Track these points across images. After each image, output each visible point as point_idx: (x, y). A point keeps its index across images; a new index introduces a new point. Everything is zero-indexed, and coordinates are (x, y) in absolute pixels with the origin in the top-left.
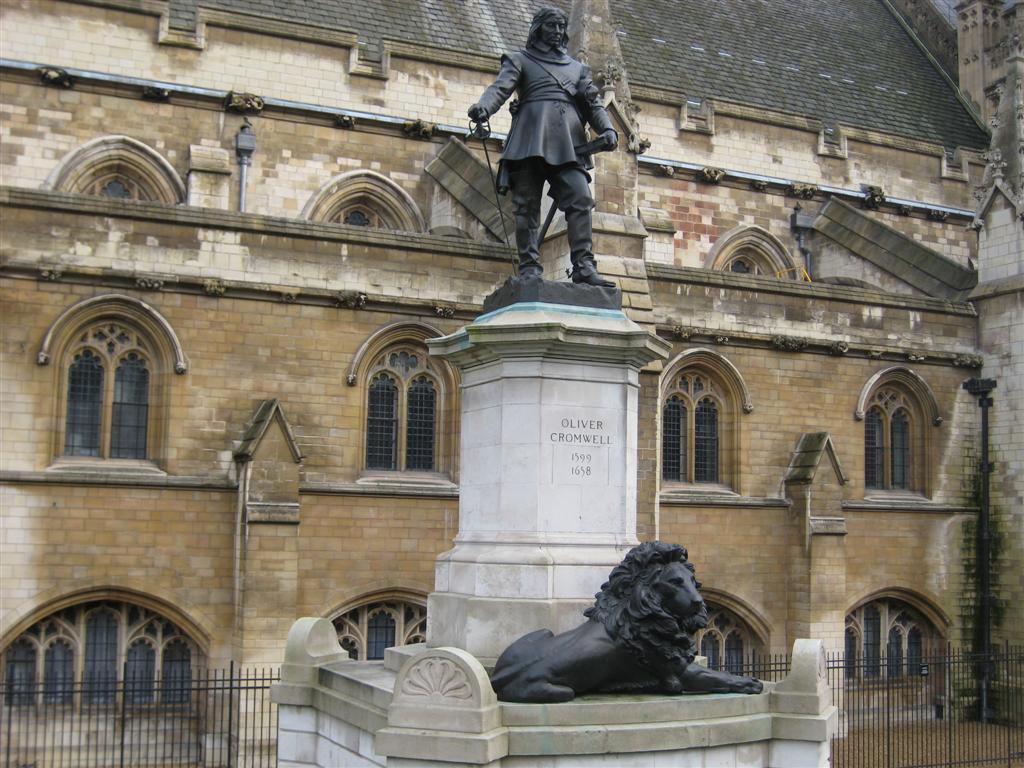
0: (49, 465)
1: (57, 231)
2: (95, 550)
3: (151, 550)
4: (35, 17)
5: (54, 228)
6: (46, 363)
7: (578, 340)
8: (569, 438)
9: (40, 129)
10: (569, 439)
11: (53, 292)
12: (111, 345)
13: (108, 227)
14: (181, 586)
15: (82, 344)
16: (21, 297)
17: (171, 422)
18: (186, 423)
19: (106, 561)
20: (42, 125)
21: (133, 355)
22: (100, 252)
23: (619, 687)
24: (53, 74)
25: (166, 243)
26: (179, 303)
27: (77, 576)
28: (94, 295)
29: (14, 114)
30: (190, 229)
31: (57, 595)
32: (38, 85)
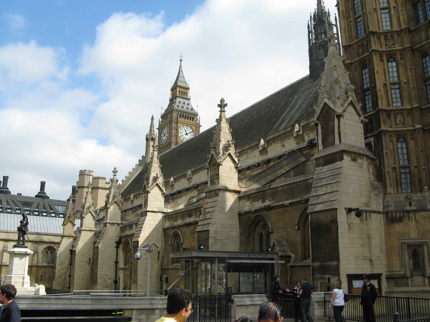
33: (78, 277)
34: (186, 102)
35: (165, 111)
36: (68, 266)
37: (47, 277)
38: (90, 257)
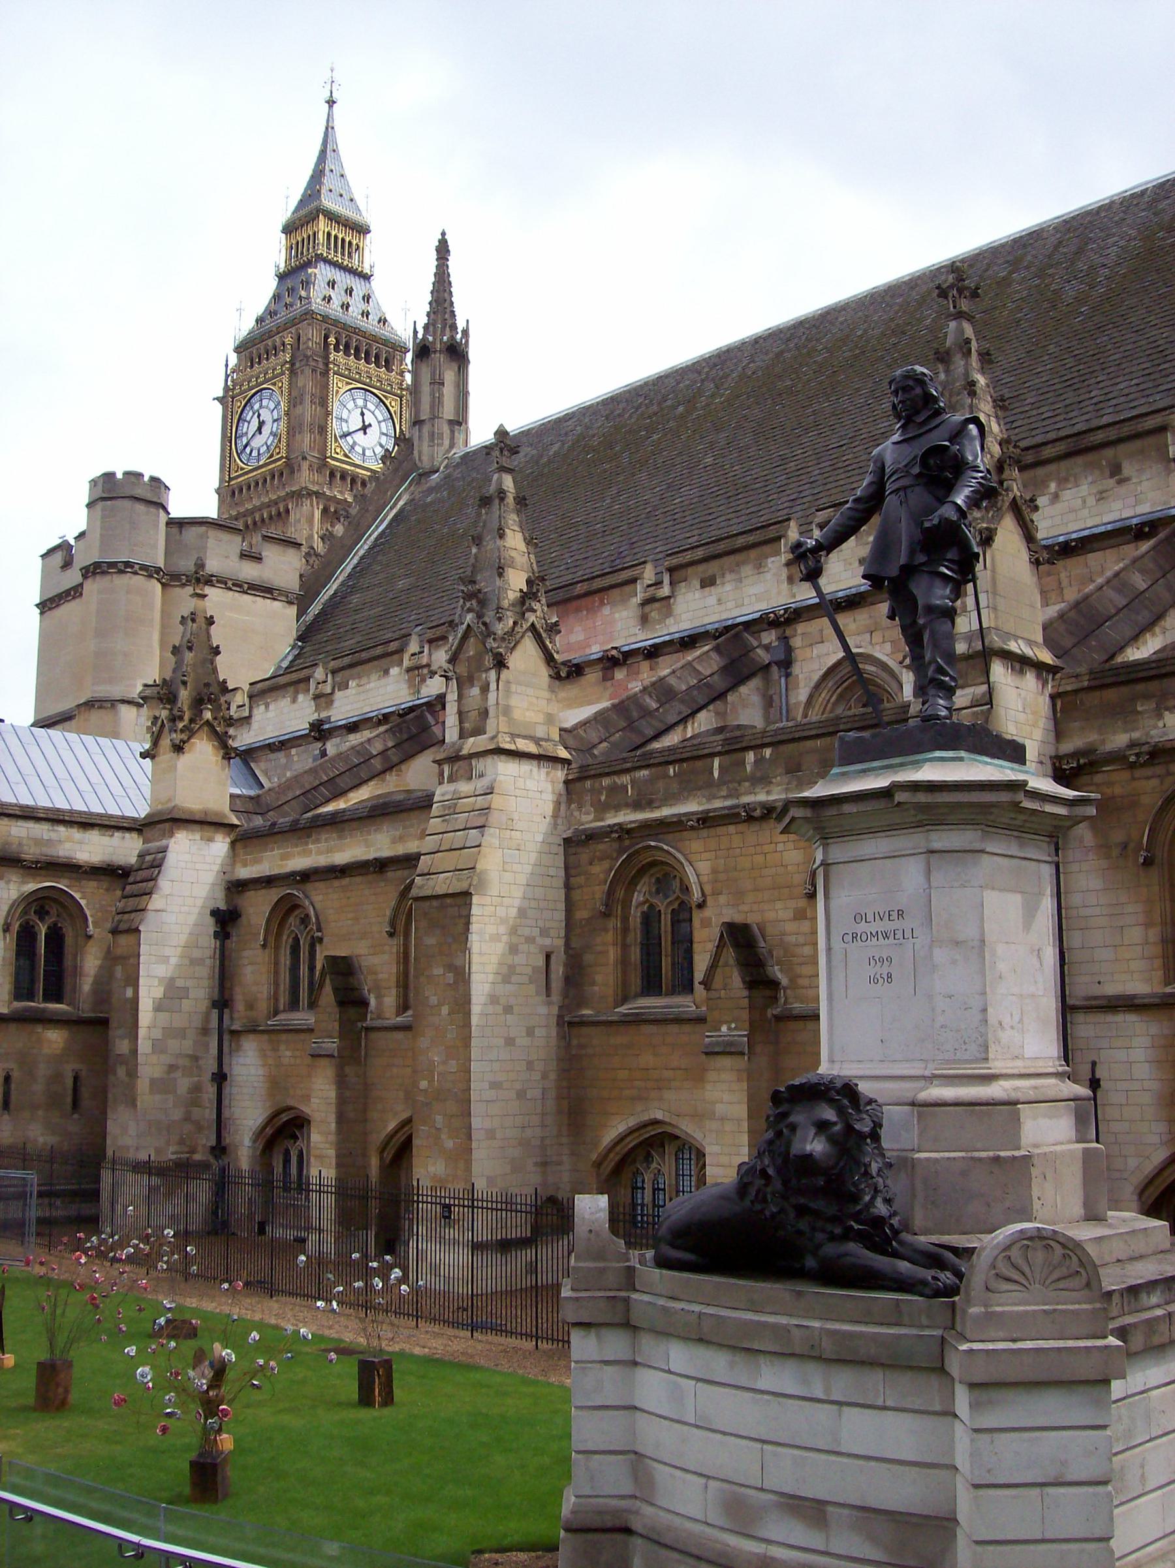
0: (1166, 985)
6: (1148, 863)
8: (864, 938)
10: (864, 938)
11: (1148, 778)
16: (1118, 790)
33: (495, 1085)
34: (359, 287)
35: (260, 320)
36: (207, 1018)
37: (39, 1087)
38: (547, 942)
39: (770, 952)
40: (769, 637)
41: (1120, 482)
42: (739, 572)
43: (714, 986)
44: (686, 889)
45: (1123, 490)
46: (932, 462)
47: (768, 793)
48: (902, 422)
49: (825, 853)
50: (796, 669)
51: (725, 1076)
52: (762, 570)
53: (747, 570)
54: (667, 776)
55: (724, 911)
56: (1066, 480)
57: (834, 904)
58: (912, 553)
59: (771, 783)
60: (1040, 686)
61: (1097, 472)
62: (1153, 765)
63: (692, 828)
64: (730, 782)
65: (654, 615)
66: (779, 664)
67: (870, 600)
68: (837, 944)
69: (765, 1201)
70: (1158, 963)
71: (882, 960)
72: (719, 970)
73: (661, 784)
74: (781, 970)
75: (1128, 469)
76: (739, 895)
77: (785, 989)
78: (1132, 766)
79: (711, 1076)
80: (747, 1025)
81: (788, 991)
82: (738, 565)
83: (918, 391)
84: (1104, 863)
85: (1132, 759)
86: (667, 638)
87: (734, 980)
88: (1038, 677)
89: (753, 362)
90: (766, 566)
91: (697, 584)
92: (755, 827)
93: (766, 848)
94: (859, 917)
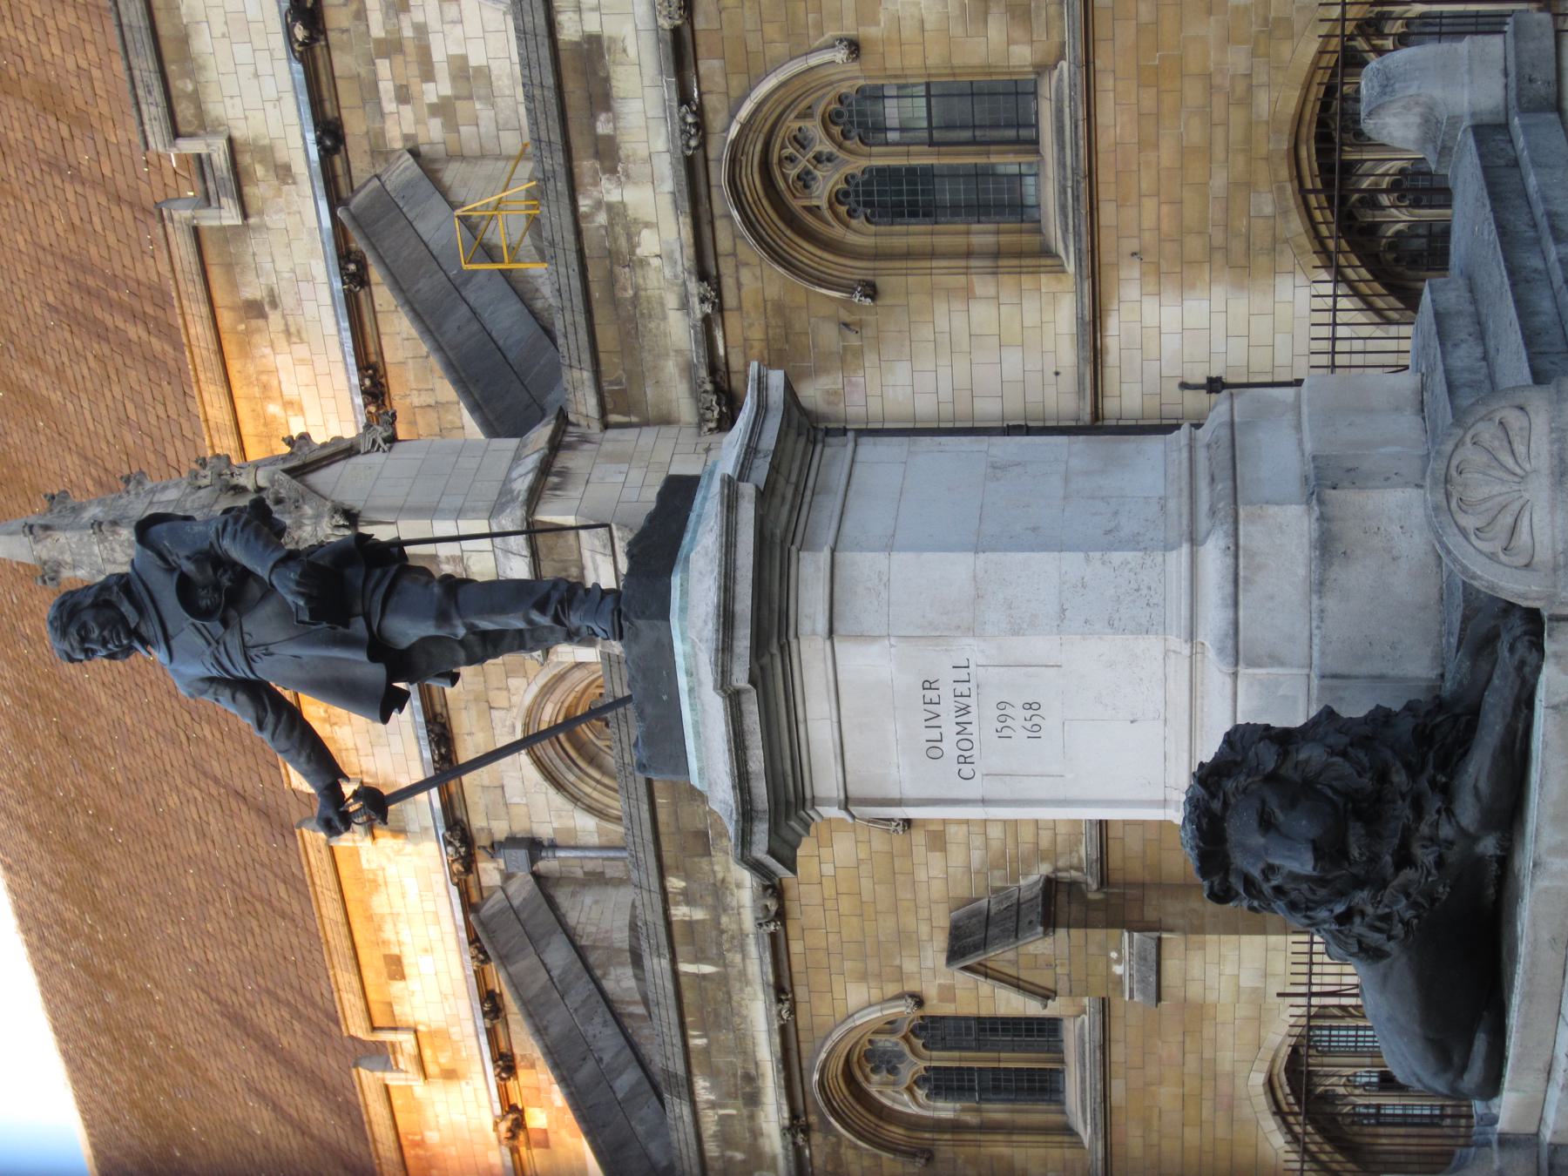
1: (625, 290)
2: (1219, 180)
3: (1217, 80)
4: (202, 68)
5: (620, 294)
6: (871, 291)
7: (760, 789)
8: (966, 745)
9: (408, 32)
10: (966, 745)
11: (739, 285)
12: (818, 158)
13: (599, 204)
14: (1288, 20)
15: (827, 214)
16: (756, 334)
17: (956, 61)
18: (957, 30)
19: (1240, 161)
20: (400, 29)
21: (830, 119)
22: (647, 213)
23: (1491, 891)
24: (300, 32)
25: (602, 98)
26: (716, 63)
27: (1268, 210)
28: (730, 217)
29: (393, 78)
30: (564, 56)
31: (1305, 242)
32: (327, 46)
39: (996, 891)
40: (489, 872)
41: (274, 304)
42: (382, 916)
43: (1051, 985)
44: (891, 1026)
45: (287, 301)
46: (204, 603)
47: (738, 886)
48: (136, 644)
49: (828, 802)
50: (544, 831)
51: (1195, 970)
52: (380, 880)
53: (379, 904)
54: (706, 1050)
55: (929, 963)
56: (265, 387)
57: (910, 792)
58: (348, 642)
59: (723, 881)
60: (587, 446)
61: (257, 339)
62: (718, 277)
63: (793, 1011)
64: (719, 945)
65: (444, 1059)
66: (533, 860)
67: (438, 709)
68: (972, 790)
69: (1386, 918)
70: (1027, 281)
71: (1003, 718)
72: (1024, 975)
73: (720, 1060)
74: (1026, 875)
75: (253, 290)
76: (904, 939)
77: (1056, 870)
78: (720, 308)
79: (1194, 991)
80: (1116, 932)
81: (1061, 864)
82: (370, 918)
83: (87, 616)
84: (870, 359)
85: (708, 308)
86: (484, 1039)
87: (1041, 950)
88: (570, 447)
89: (41, 875)
90: (374, 872)
91: (397, 987)
92: (793, 908)
93: (829, 891)
94: (934, 750)
